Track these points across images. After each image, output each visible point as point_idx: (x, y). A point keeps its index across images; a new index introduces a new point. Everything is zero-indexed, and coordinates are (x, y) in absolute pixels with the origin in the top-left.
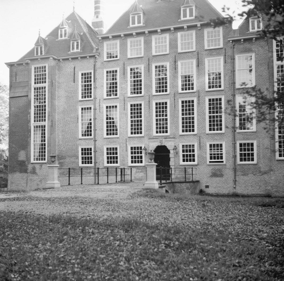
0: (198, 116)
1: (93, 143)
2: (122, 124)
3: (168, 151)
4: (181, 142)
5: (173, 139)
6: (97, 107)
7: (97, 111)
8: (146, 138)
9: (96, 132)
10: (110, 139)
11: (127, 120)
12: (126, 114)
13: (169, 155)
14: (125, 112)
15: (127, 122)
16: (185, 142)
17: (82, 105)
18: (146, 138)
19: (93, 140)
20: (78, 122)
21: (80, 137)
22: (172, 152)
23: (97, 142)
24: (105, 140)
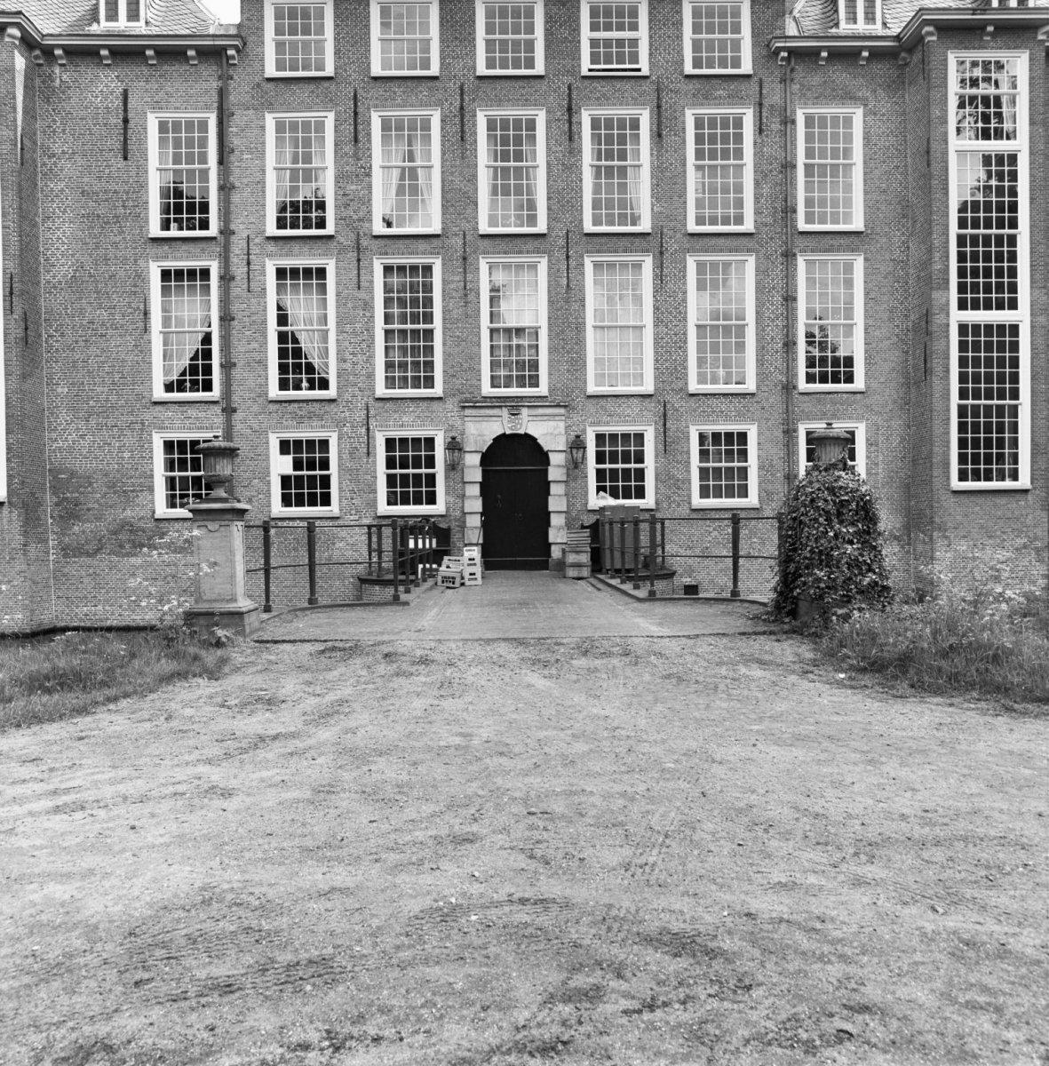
0: (656, 326)
1: (219, 420)
2: (347, 343)
3: (542, 457)
4: (593, 424)
5: (562, 411)
6: (239, 270)
7: (238, 289)
8: (451, 405)
9: (236, 373)
10: (296, 405)
11: (370, 330)
12: (368, 306)
13: (547, 471)
14: (362, 295)
15: (372, 337)
16: (607, 424)
17: (166, 258)
18: (451, 405)
19: (217, 409)
20: (146, 330)
21: (159, 393)
22: (556, 459)
23: (238, 416)
24: (277, 406)
